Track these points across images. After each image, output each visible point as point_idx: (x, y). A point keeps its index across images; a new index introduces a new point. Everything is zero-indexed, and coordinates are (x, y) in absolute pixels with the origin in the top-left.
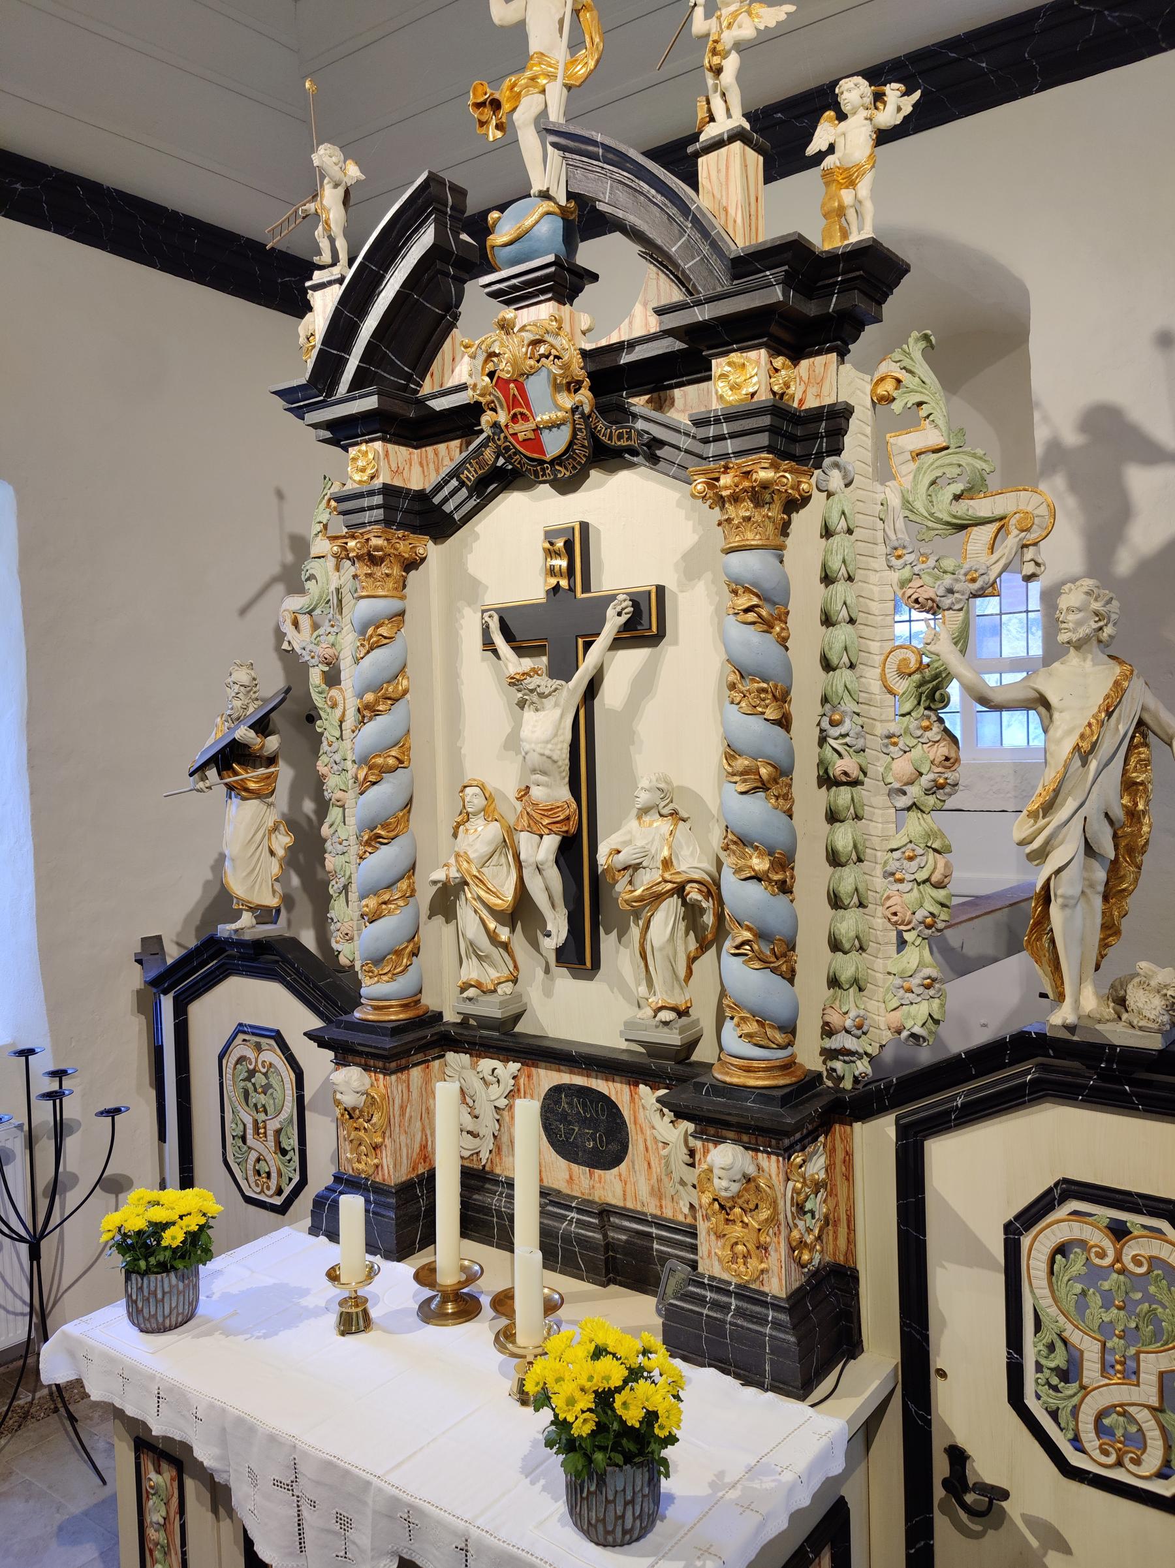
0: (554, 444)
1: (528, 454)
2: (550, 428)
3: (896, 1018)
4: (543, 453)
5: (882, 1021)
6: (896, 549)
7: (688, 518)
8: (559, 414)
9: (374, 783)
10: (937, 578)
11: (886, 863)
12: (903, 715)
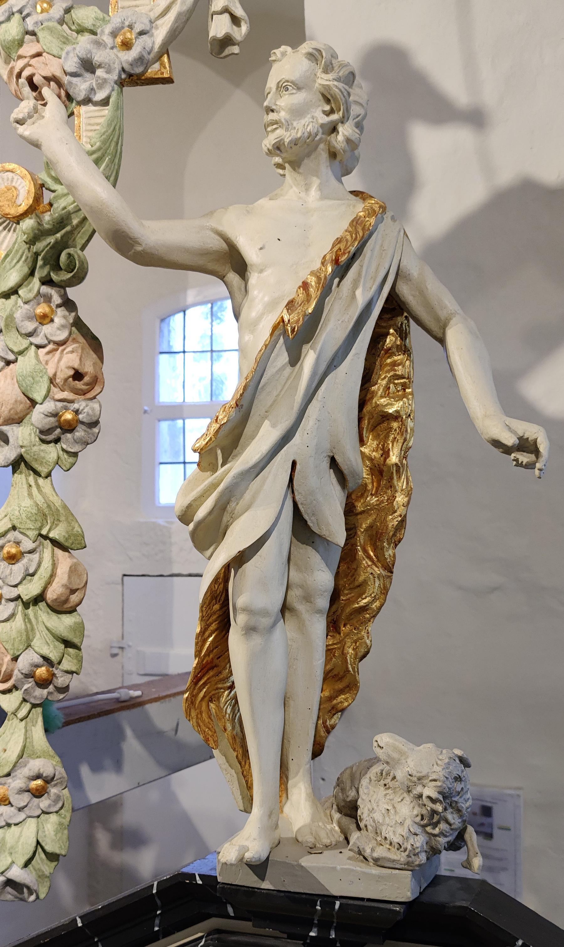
10: (66, 41)
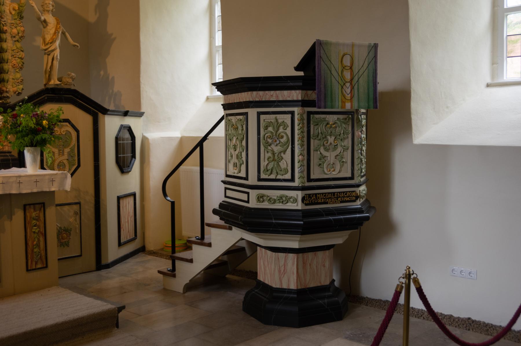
3: (15, 89)
5: (11, 90)
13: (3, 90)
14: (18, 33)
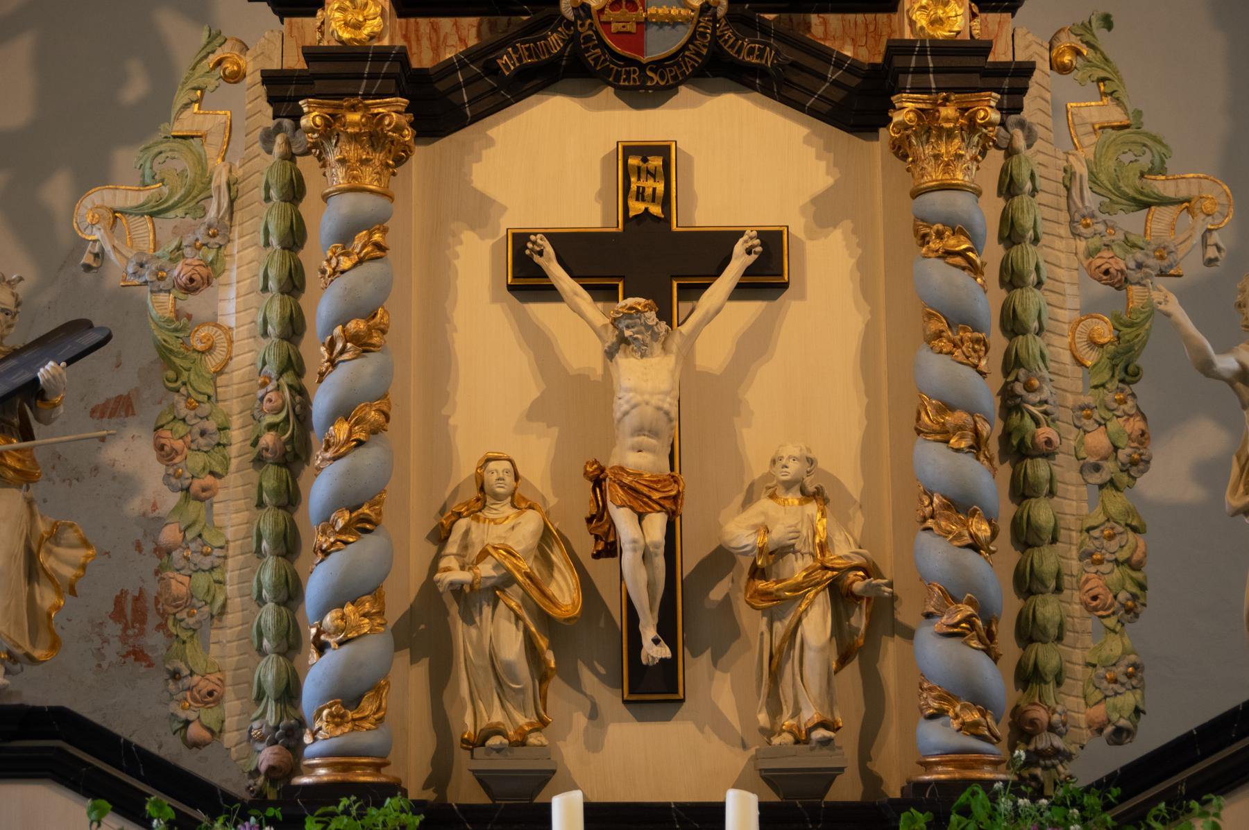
0: (659, 46)
1: (618, 50)
2: (661, 24)
3: (1099, 712)
4: (641, 52)
5: (1082, 719)
6: (1084, 217)
7: (819, 157)
8: (683, 12)
9: (360, 443)
10: (1127, 252)
11: (1082, 543)
12: (1096, 387)
13: (1033, 722)
14: (1116, 448)
